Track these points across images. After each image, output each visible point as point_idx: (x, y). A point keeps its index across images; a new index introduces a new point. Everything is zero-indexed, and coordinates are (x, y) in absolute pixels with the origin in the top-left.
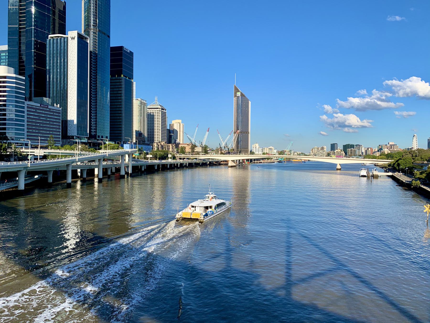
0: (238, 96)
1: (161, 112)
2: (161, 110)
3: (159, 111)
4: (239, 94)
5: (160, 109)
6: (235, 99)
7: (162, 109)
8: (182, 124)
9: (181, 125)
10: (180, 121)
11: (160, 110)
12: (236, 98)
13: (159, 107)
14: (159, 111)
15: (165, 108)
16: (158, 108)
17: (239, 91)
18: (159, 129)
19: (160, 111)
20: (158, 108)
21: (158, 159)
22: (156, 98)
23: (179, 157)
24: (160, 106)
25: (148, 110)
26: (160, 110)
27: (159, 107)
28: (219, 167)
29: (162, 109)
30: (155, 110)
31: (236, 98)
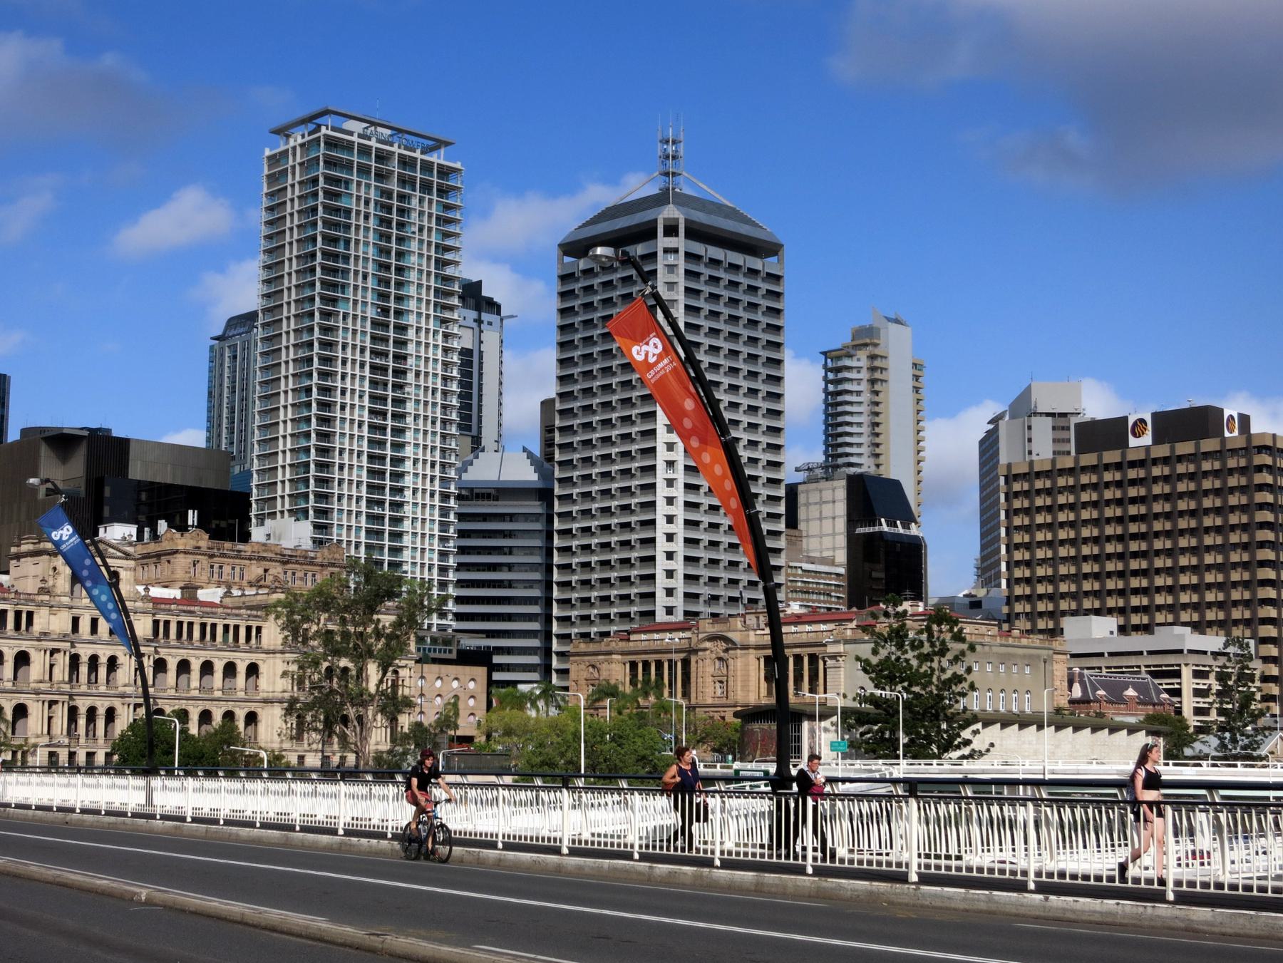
5: (671, 230)
11: (671, 242)
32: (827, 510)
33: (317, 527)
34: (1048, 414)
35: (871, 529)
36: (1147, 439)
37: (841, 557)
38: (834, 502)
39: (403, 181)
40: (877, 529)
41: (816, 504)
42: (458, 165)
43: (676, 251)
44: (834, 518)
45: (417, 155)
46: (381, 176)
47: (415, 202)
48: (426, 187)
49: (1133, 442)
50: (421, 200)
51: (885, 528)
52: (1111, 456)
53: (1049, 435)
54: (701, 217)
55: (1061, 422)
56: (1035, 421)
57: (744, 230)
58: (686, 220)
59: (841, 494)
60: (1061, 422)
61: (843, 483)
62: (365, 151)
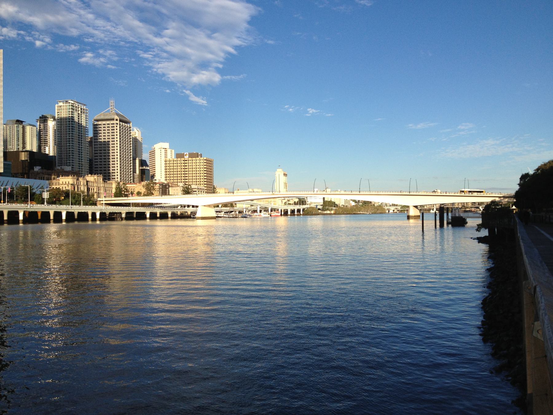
2: (118, 122)
3: (115, 125)
5: (117, 120)
7: (120, 121)
8: (170, 150)
9: (169, 151)
10: (166, 145)
11: (117, 122)
14: (115, 125)
15: (128, 118)
16: (113, 119)
19: (117, 124)
22: (112, 102)
23: (104, 202)
24: (118, 115)
26: (117, 122)
27: (116, 117)
29: (120, 121)
30: (108, 122)
33: (72, 168)
35: (142, 168)
36: (187, 157)
39: (81, 112)
40: (143, 168)
42: (87, 109)
43: (117, 124)
47: (83, 115)
49: (185, 157)
51: (145, 168)
52: (183, 159)
53: (164, 152)
54: (122, 118)
55: (166, 150)
57: (126, 120)
60: (166, 150)
62: (76, 107)
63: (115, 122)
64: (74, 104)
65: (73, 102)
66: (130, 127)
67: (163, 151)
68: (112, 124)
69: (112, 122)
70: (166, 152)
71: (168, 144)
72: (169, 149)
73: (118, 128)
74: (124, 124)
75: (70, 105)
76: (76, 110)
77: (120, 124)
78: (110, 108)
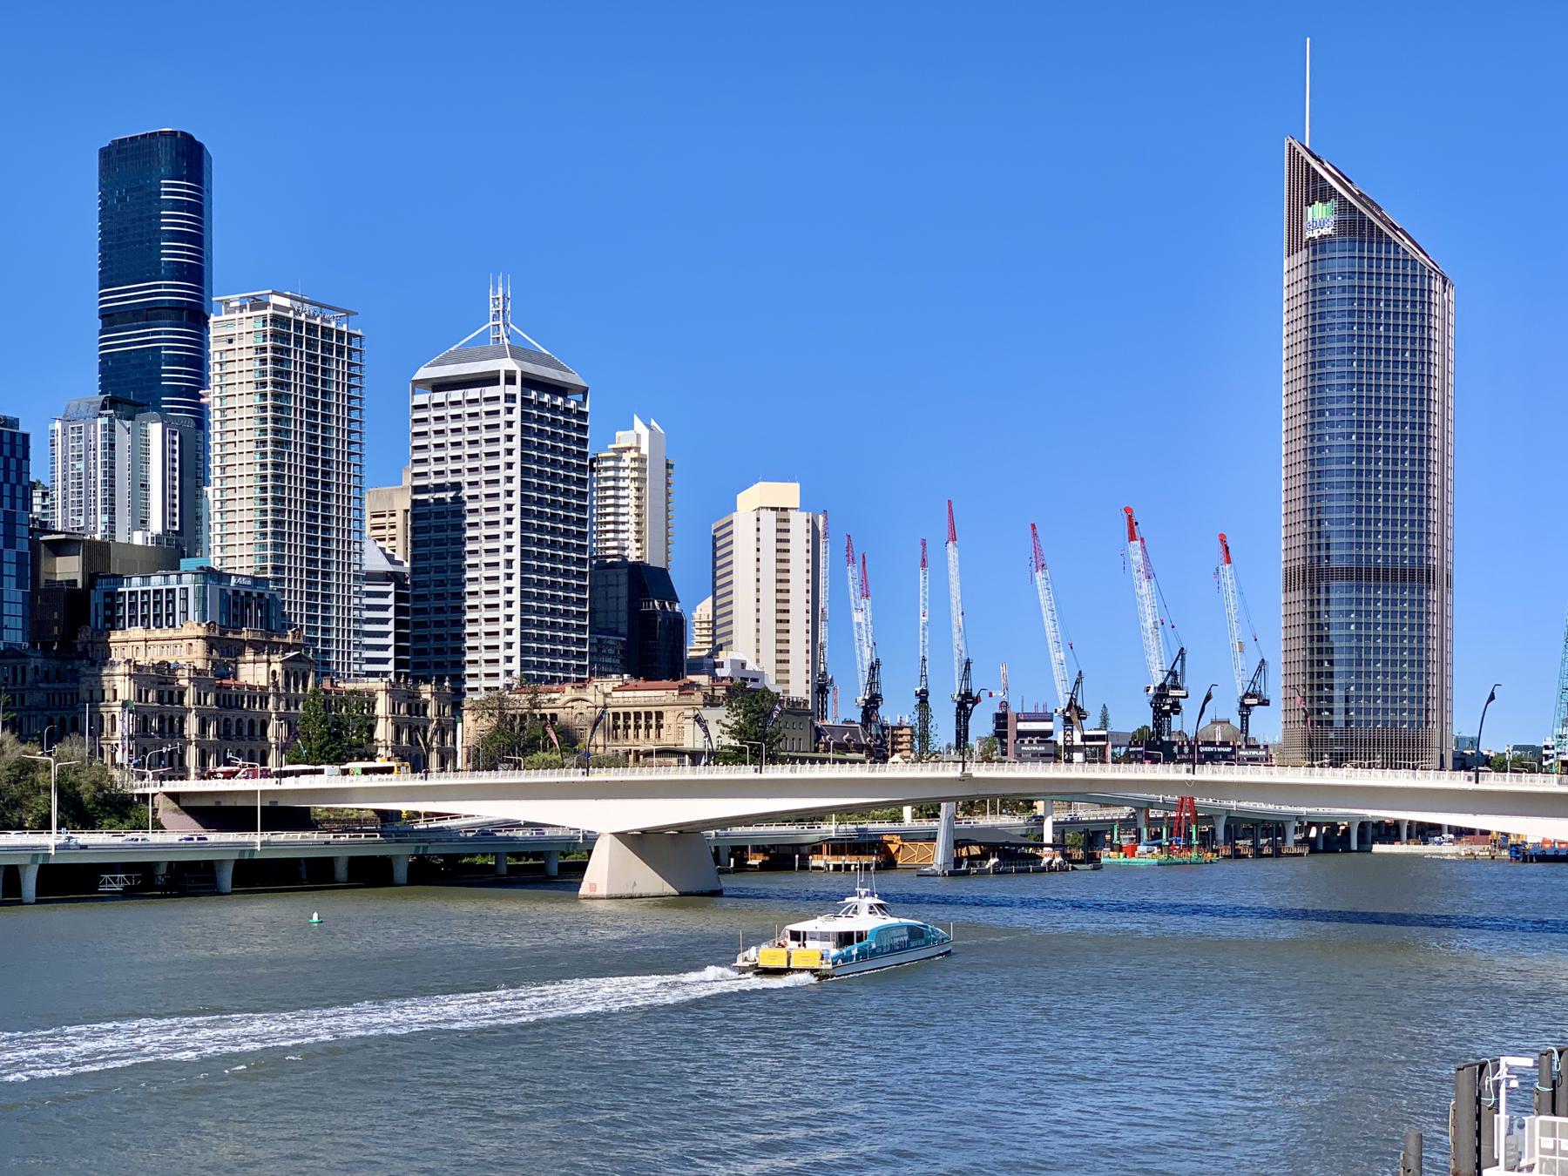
0: (1316, 235)
1: (518, 406)
2: (516, 389)
3: (501, 406)
4: (1321, 219)
5: (510, 380)
6: (1292, 270)
10: (788, 493)
11: (511, 389)
12: (1302, 256)
13: (506, 364)
14: (501, 406)
17: (1325, 194)
18: (501, 558)
19: (510, 398)
20: (491, 379)
21: (150, 830)
24: (516, 354)
25: (421, 399)
26: (511, 389)
28: (214, 898)
30: (473, 393)
31: (1302, 256)
32: (612, 591)
34: (773, 509)
37: (623, 628)
38: (618, 586)
39: (327, 348)
41: (603, 586)
42: (359, 332)
43: (514, 396)
44: (617, 599)
45: (333, 325)
46: (311, 344)
48: (340, 352)
50: (338, 361)
54: (533, 369)
55: (783, 515)
56: (763, 512)
58: (522, 372)
59: (624, 580)
60: (783, 515)
61: (626, 571)
62: (298, 325)
63: (498, 390)
64: (287, 310)
65: (286, 302)
66: (582, 415)
67: (770, 519)
68: (487, 400)
69: (490, 391)
70: (783, 526)
71: (798, 485)
72: (801, 509)
73: (516, 416)
74: (546, 398)
75: (265, 316)
76: (298, 341)
77: (526, 402)
78: (491, 323)
